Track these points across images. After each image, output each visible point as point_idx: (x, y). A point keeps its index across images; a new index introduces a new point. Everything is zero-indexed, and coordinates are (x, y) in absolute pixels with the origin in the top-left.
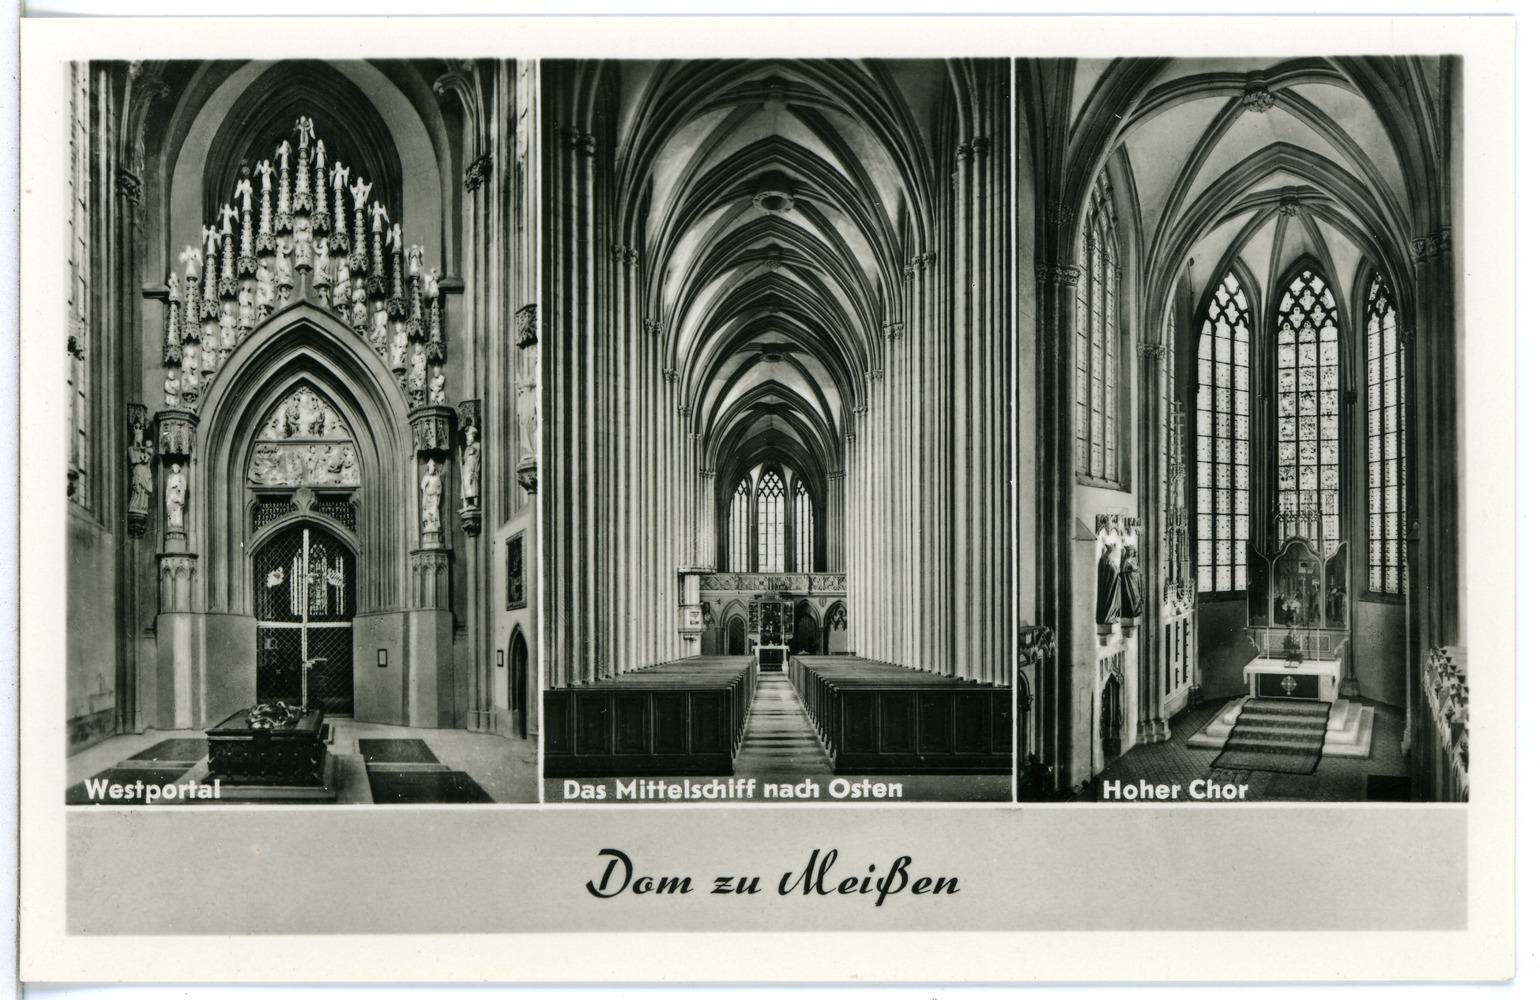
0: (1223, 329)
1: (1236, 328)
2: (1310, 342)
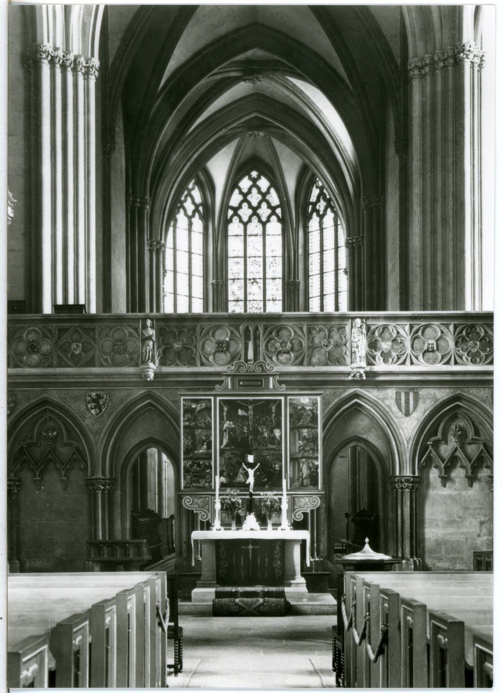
0: (181, 217)
1: (193, 220)
2: (256, 235)
